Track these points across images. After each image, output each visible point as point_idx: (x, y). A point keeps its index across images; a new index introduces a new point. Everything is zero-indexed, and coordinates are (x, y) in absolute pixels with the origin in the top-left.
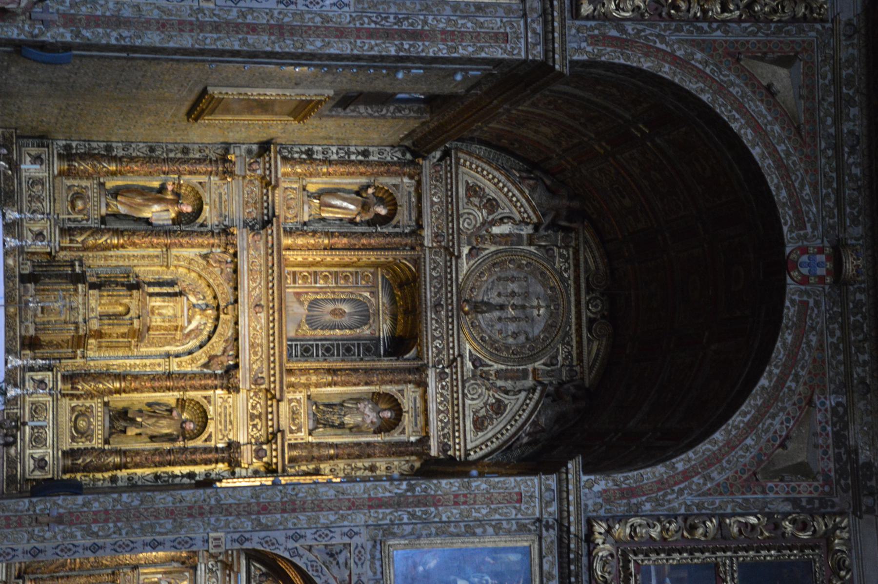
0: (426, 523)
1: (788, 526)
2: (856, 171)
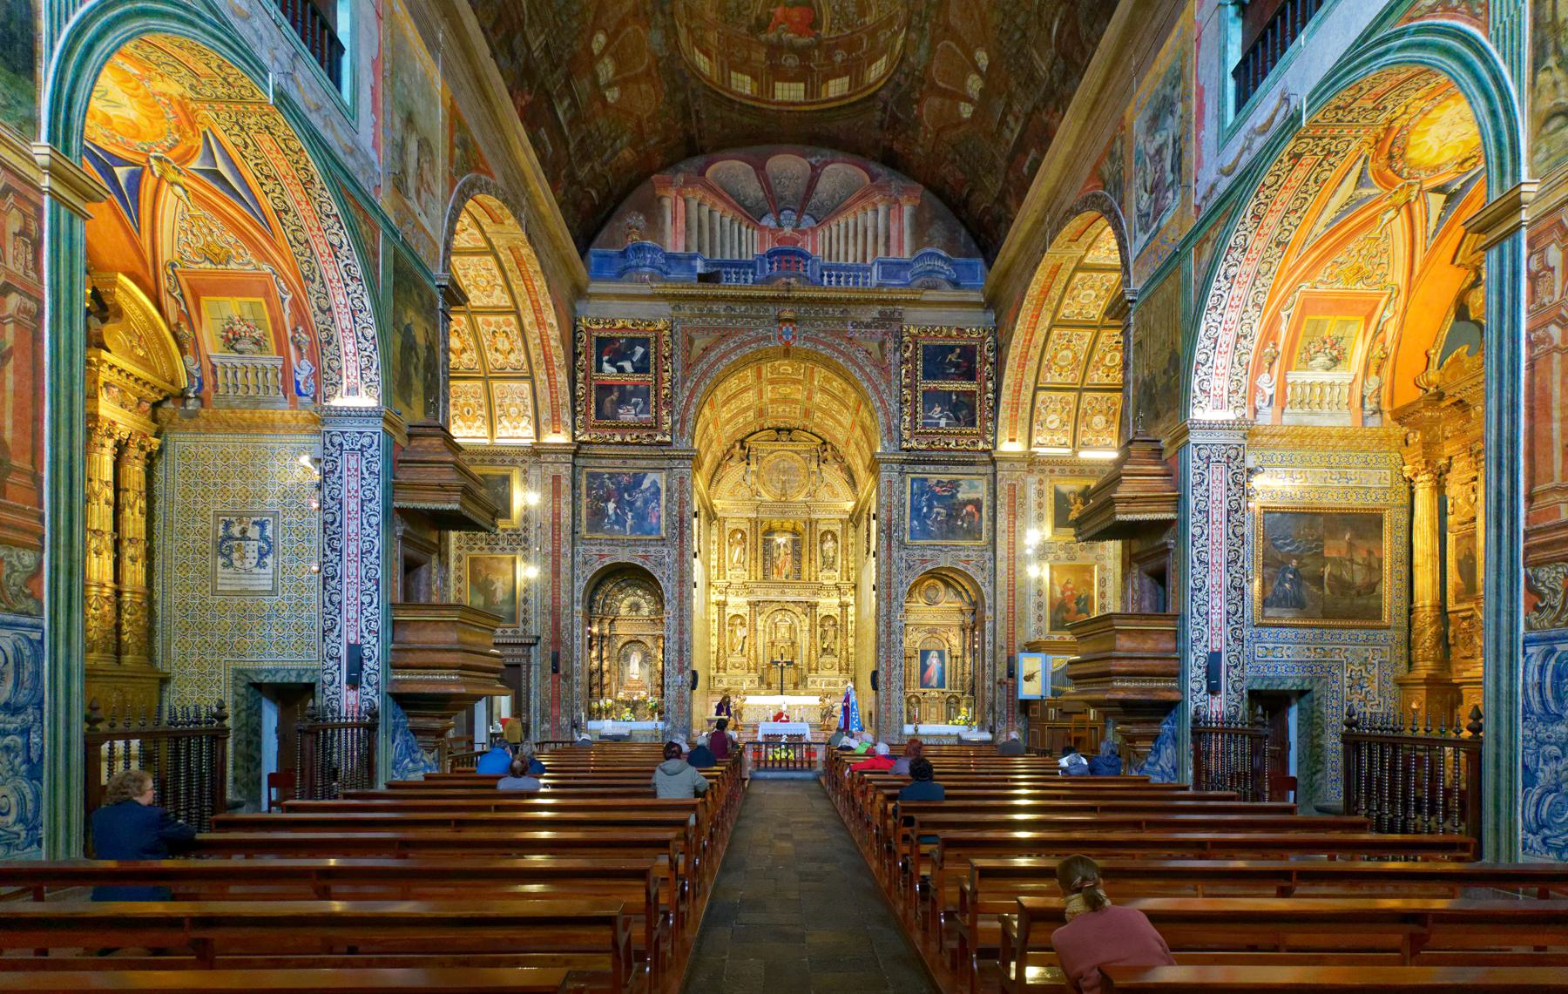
0: (898, 525)
1: (907, 355)
2: (743, 308)
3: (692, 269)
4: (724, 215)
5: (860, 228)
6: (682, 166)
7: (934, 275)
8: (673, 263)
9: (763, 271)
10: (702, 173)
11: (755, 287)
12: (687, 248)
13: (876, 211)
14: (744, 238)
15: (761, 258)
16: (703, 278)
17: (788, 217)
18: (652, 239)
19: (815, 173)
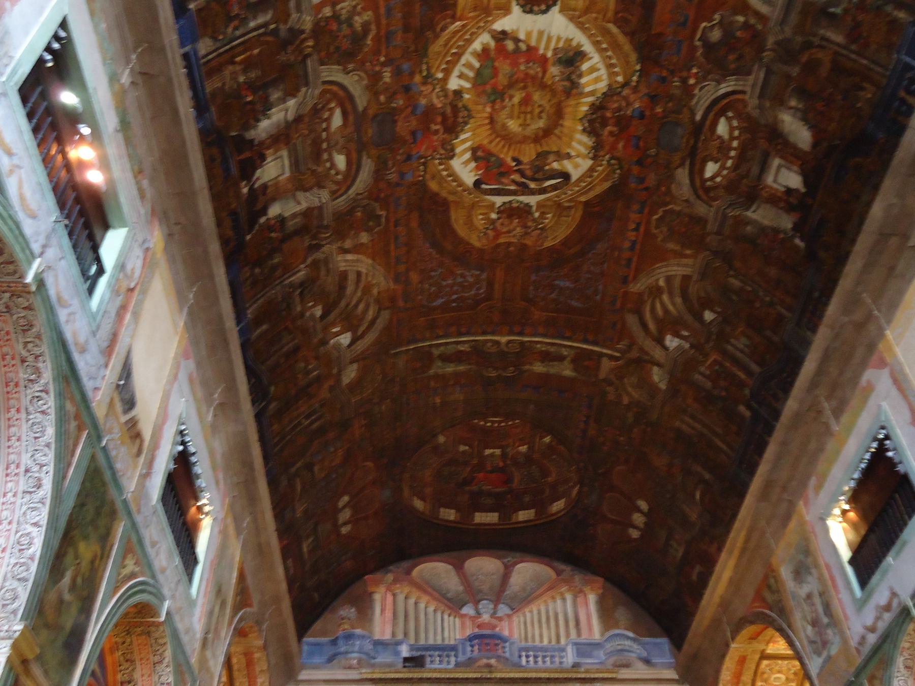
3: (397, 653)
4: (427, 606)
5: (551, 614)
6: (391, 568)
7: (626, 653)
8: (380, 648)
9: (464, 653)
10: (408, 572)
11: (459, 669)
12: (394, 634)
13: (564, 599)
14: (446, 625)
15: (463, 641)
16: (406, 660)
17: (486, 607)
18: (363, 628)
19: (508, 570)
